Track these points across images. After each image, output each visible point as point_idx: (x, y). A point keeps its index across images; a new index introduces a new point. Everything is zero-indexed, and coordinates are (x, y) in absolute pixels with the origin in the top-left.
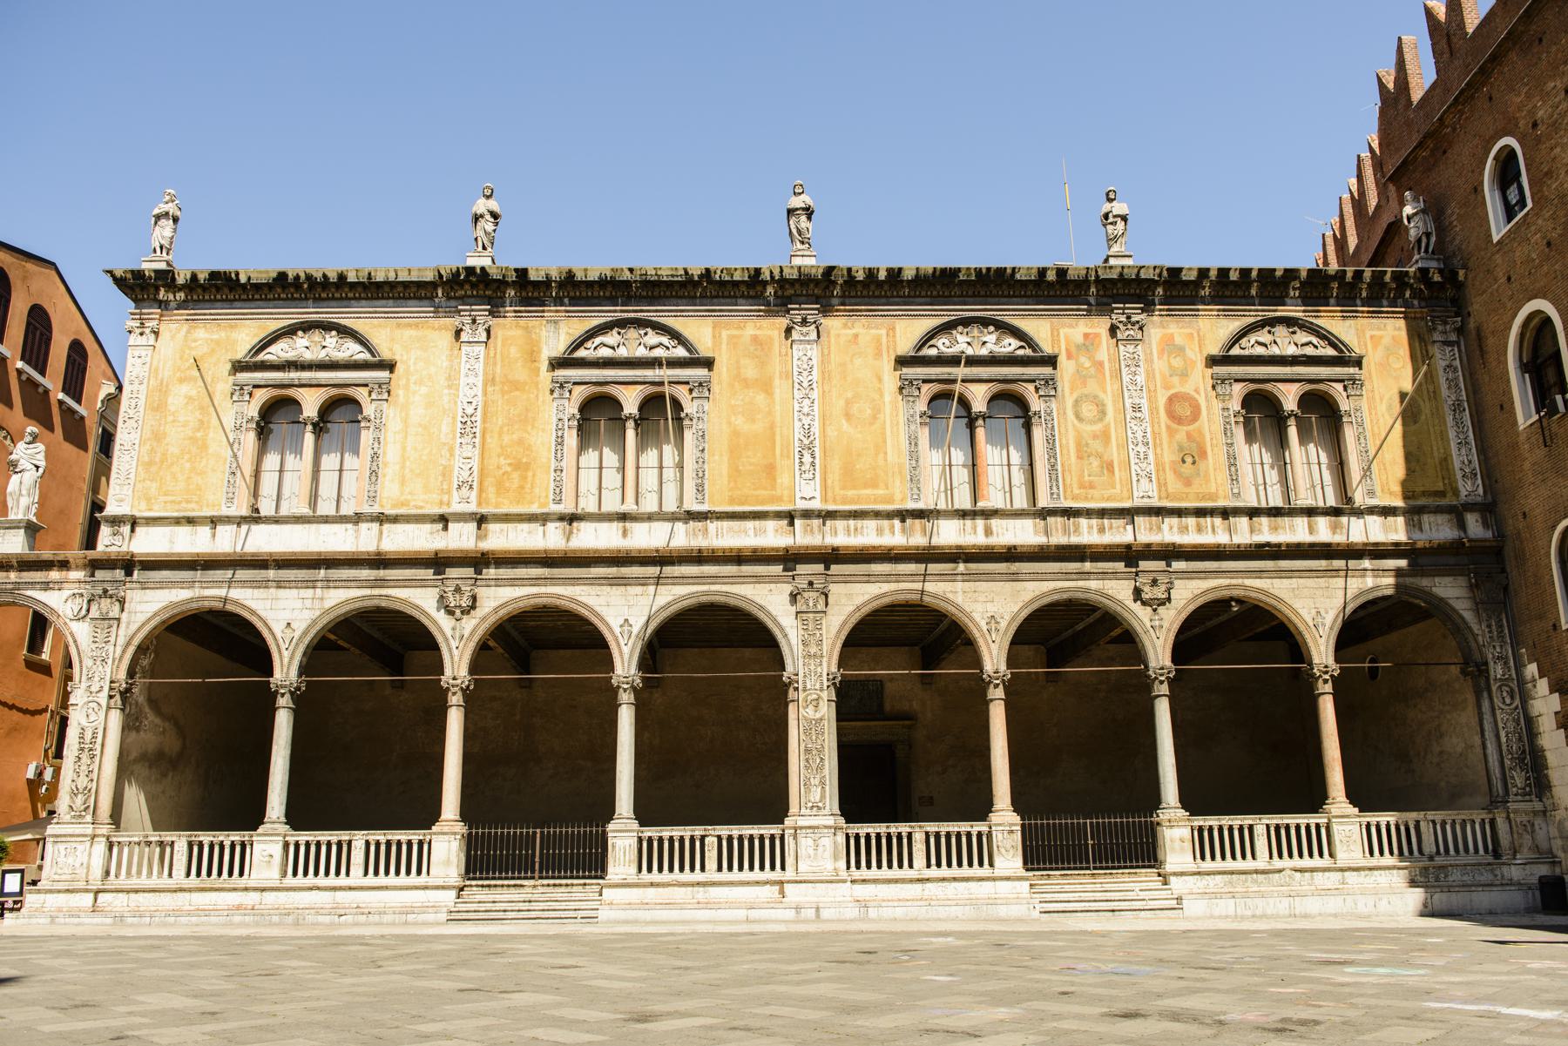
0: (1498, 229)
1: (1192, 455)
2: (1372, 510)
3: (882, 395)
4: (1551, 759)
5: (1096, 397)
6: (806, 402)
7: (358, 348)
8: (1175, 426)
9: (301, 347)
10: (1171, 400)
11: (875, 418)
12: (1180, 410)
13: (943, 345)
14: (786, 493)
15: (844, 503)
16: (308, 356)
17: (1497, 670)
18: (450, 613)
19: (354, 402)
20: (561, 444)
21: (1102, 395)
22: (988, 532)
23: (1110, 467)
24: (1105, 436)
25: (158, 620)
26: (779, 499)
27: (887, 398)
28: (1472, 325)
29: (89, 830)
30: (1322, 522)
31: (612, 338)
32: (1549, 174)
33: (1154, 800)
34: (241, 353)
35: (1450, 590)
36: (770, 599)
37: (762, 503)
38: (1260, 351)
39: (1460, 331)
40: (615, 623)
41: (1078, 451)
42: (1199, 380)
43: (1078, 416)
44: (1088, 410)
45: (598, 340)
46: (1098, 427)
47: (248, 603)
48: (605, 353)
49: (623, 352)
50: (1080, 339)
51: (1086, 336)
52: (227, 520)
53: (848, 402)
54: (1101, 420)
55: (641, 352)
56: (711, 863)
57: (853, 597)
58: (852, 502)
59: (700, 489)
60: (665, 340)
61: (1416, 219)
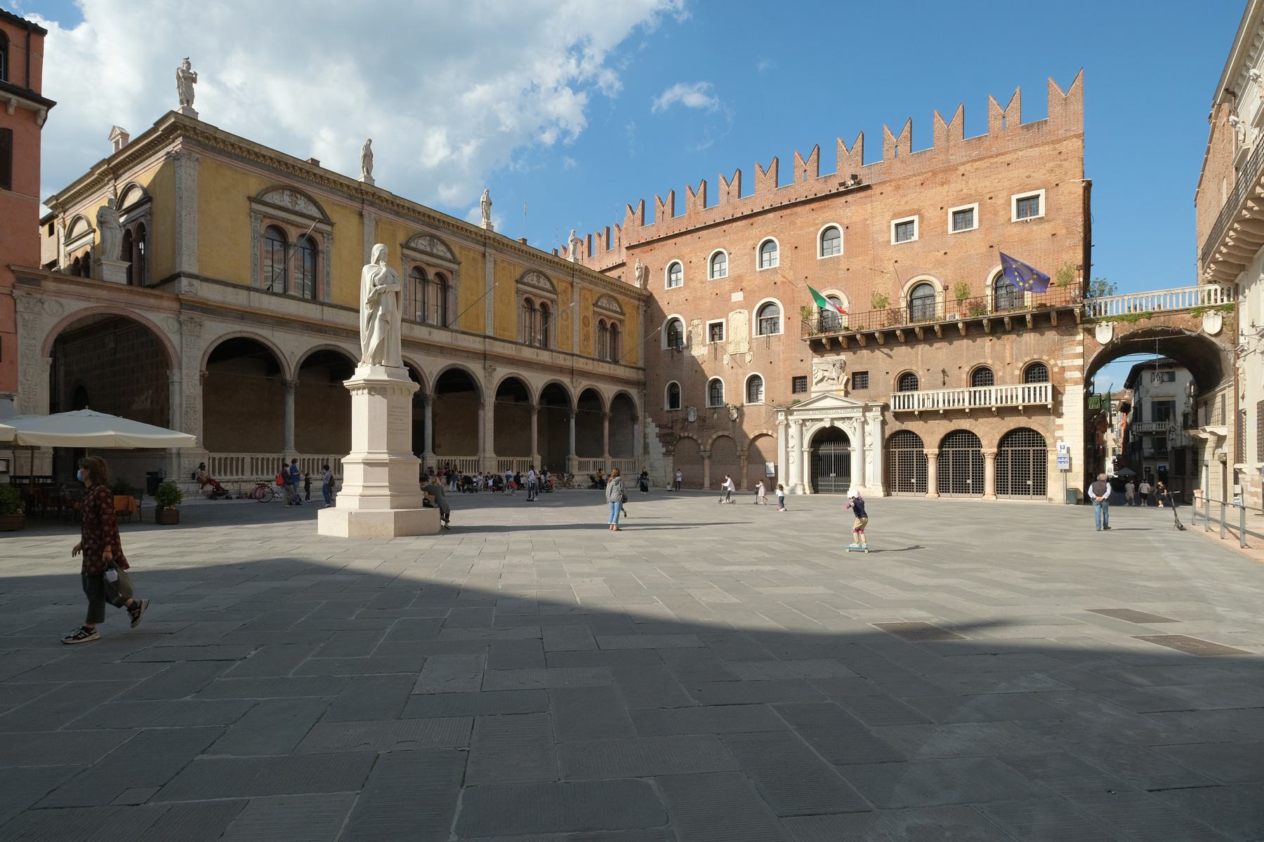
1: (587, 338)
9: (285, 200)
17: (641, 418)
25: (221, 341)
33: (568, 452)
34: (253, 194)
35: (633, 392)
36: (476, 368)
40: (427, 372)
42: (590, 314)
48: (422, 247)
49: (428, 249)
52: (257, 290)
55: (435, 251)
57: (502, 372)
60: (444, 249)
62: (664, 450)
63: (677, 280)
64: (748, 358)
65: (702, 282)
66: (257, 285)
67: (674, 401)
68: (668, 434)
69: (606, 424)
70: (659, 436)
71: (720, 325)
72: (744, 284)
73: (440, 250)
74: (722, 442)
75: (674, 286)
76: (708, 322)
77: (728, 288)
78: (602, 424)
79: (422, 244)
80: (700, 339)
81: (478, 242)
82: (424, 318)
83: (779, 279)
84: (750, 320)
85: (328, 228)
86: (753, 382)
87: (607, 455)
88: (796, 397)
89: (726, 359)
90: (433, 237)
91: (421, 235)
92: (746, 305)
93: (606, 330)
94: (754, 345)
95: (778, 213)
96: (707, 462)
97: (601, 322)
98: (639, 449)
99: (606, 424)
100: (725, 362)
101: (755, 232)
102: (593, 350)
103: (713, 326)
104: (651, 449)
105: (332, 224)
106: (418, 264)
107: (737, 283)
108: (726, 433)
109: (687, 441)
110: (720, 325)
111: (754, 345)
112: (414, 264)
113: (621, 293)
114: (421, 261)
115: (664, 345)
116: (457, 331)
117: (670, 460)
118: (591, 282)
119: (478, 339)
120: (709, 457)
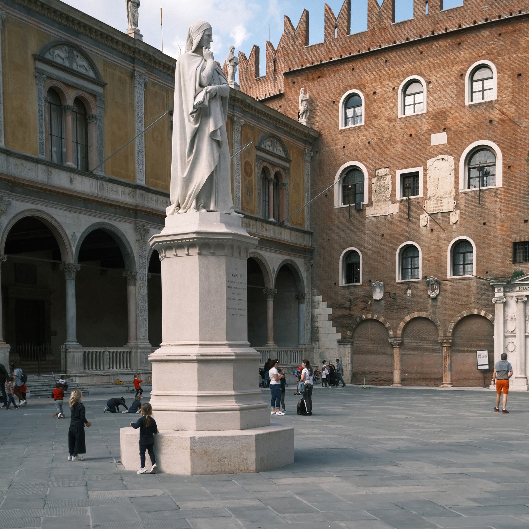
0: (341, 127)
4: (321, 330)
8: (246, 177)
17: (308, 296)
28: (317, 156)
32: (376, 116)
38: (268, 148)
39: (312, 157)
45: (57, 52)
48: (59, 61)
49: (67, 64)
55: (75, 67)
59: (101, 162)
61: (304, 103)
62: (339, 336)
63: (355, 117)
64: (454, 218)
65: (390, 120)
67: (352, 274)
68: (343, 317)
69: (271, 304)
70: (331, 318)
71: (416, 175)
72: (449, 122)
73: (80, 64)
74: (418, 326)
75: (350, 125)
76: (399, 172)
77: (425, 127)
78: (265, 302)
80: (389, 193)
81: (125, 56)
82: (62, 156)
83: (496, 115)
84: (457, 169)
86: (460, 248)
87: (271, 344)
88: (518, 268)
89: (424, 219)
90: (73, 47)
91: (58, 44)
92: (452, 148)
93: (269, 181)
94: (462, 201)
95: (496, 31)
96: (396, 351)
97: (265, 171)
98: (305, 336)
99: (271, 304)
100: (422, 223)
101: (464, 54)
103: (404, 177)
104: (322, 336)
106: (55, 83)
107: (438, 120)
108: (423, 314)
109: (369, 325)
110: (416, 175)
111: (462, 201)
112: (50, 84)
113: (285, 132)
114: (59, 80)
115: (338, 202)
116: (103, 179)
117: (347, 350)
118: (253, 117)
119: (127, 190)
120: (401, 345)
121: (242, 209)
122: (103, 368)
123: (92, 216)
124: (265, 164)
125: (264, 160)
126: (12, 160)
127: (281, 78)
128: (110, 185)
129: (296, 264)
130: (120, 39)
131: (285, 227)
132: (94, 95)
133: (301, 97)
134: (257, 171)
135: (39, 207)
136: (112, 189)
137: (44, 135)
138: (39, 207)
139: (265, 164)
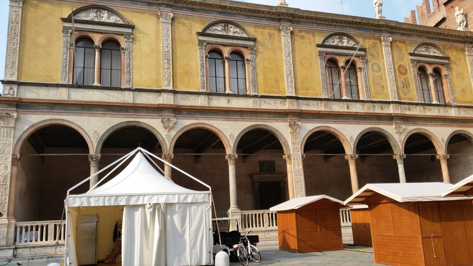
2: (454, 107)
3: (312, 58)
5: (378, 64)
6: (288, 58)
7: (118, 19)
8: (401, 75)
10: (399, 66)
11: (310, 65)
12: (401, 70)
13: (330, 42)
14: (283, 90)
15: (302, 95)
16: (96, 20)
18: (165, 128)
19: (117, 43)
20: (203, 66)
21: (379, 63)
22: (348, 107)
23: (383, 87)
24: (381, 77)
26: (281, 92)
27: (314, 59)
29: (6, 221)
30: (442, 109)
31: (219, 28)
34: (66, 16)
37: (276, 93)
40: (227, 134)
41: (373, 81)
43: (373, 70)
44: (375, 68)
45: (214, 28)
46: (379, 74)
47: (76, 122)
49: (224, 33)
50: (372, 43)
51: (374, 43)
53: (301, 60)
54: (379, 72)
56: (266, 224)
58: (305, 95)
60: (238, 30)
66: (66, 83)
79: (218, 30)
85: (129, 30)
97: (422, 70)
102: (414, 94)
105: (132, 27)
106: (214, 46)
112: (210, 47)
113: (440, 39)
118: (403, 34)
119: (279, 101)
121: (399, 98)
122: (263, 226)
123: (248, 121)
124: (420, 64)
125: (418, 62)
126: (179, 96)
127: (443, 7)
128: (263, 99)
129: (470, 133)
130: (264, 10)
131: (451, 106)
132: (246, 47)
133: (457, 12)
134: (412, 70)
135: (201, 121)
136: (265, 102)
137: (205, 77)
138: (201, 121)
139: (433, 66)
